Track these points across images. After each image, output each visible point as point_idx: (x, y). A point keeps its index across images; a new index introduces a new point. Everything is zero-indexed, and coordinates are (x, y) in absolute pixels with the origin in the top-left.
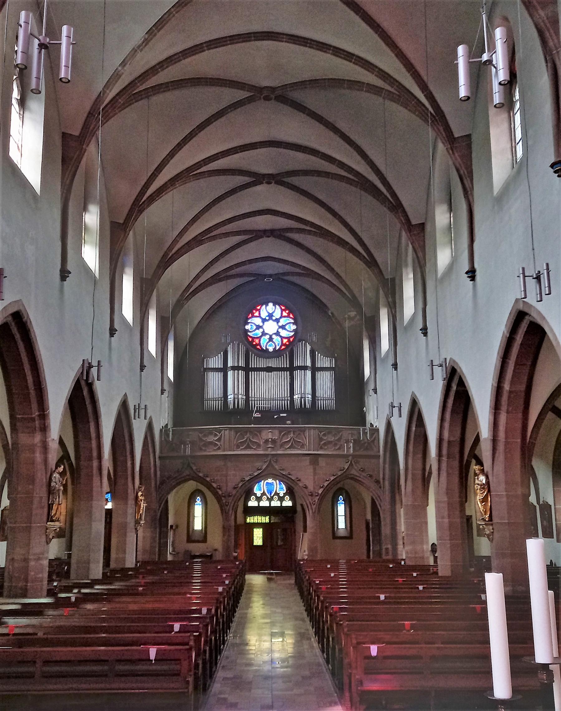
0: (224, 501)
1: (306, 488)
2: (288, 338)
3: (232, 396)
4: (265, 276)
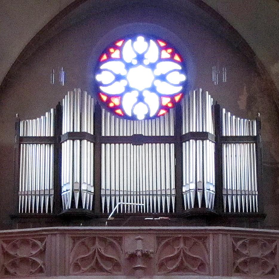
2: (172, 97)
3: (70, 187)
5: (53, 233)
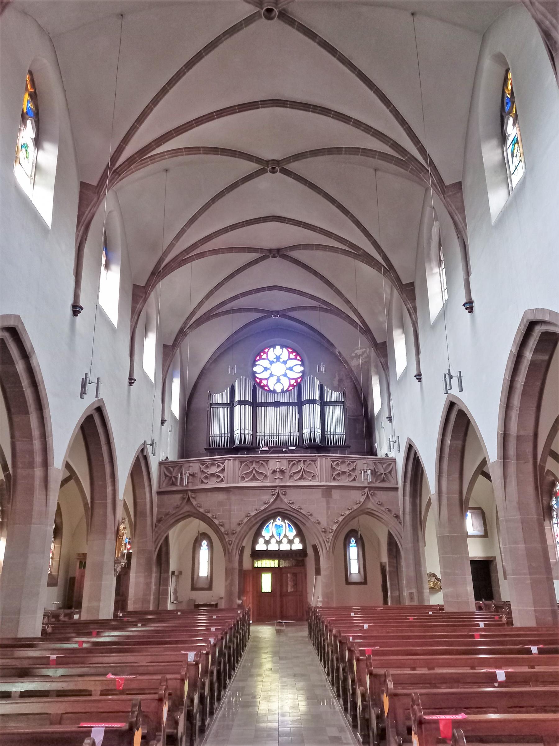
0: (227, 540)
1: (319, 523)
2: (296, 379)
3: (239, 431)
4: (272, 312)
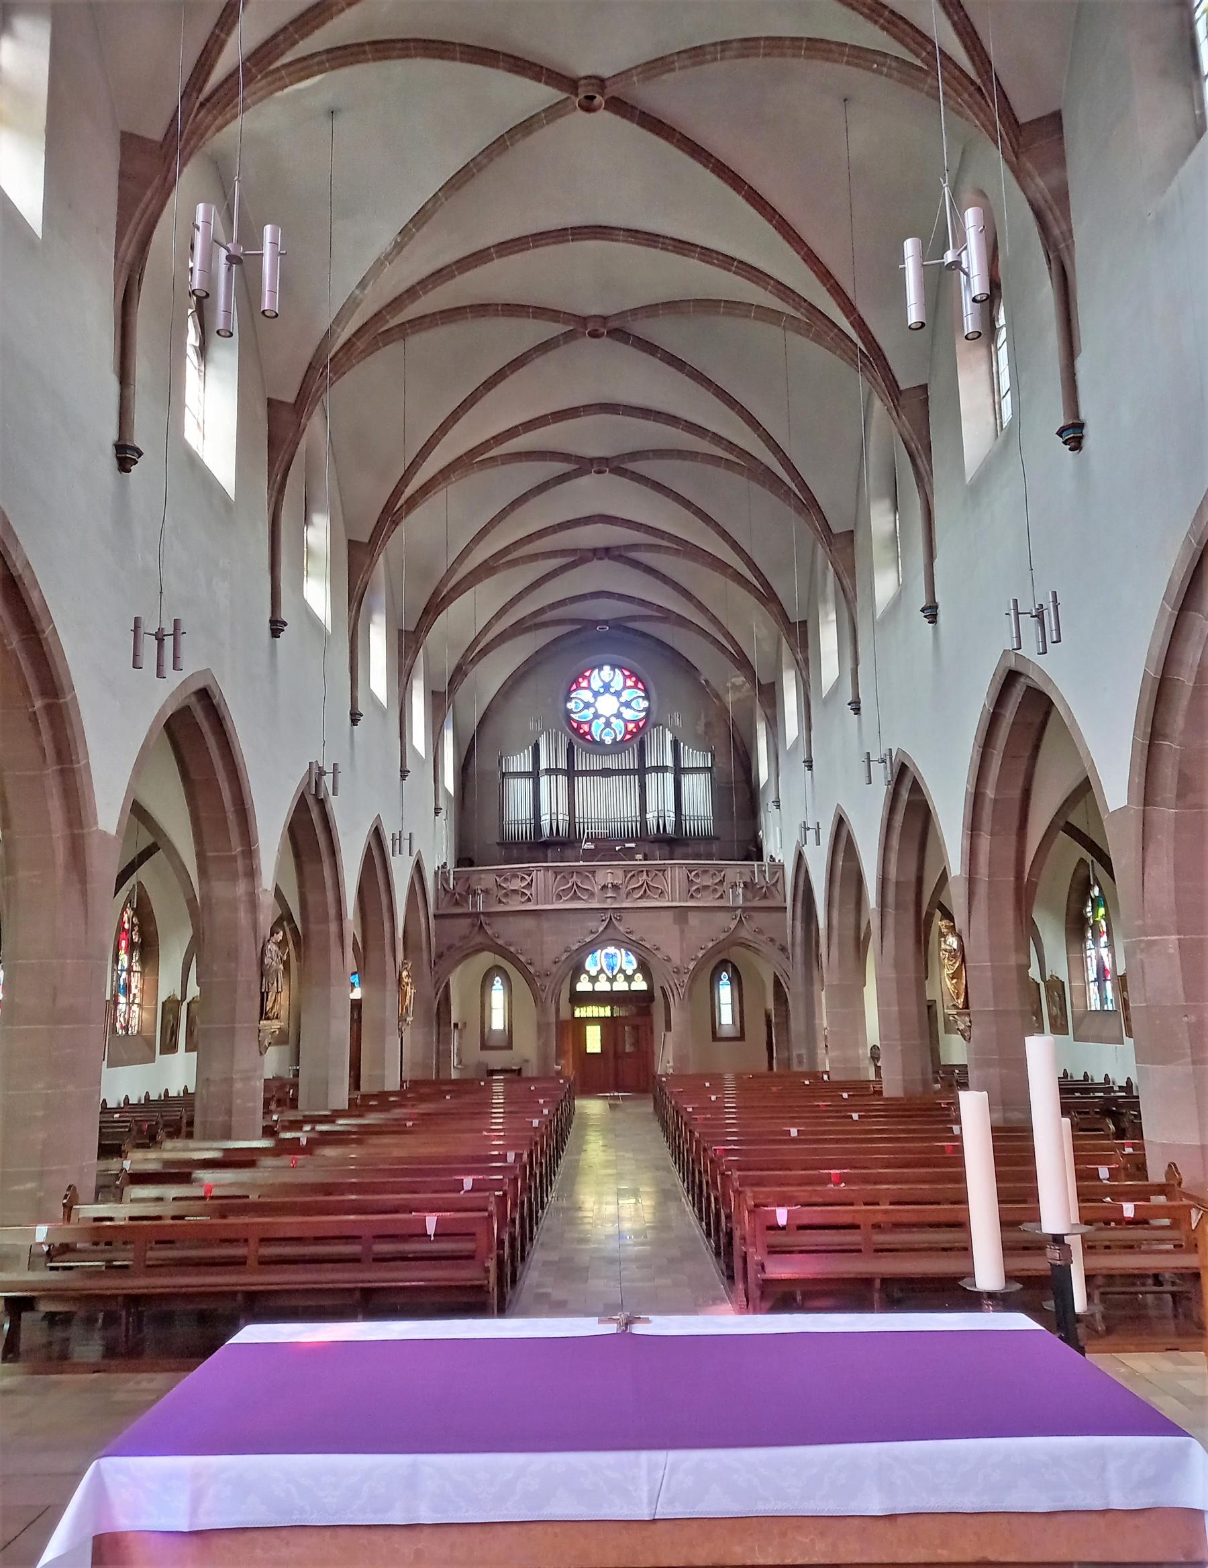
1: (669, 960)
2: (636, 722)
4: (597, 623)
5: (538, 869)
